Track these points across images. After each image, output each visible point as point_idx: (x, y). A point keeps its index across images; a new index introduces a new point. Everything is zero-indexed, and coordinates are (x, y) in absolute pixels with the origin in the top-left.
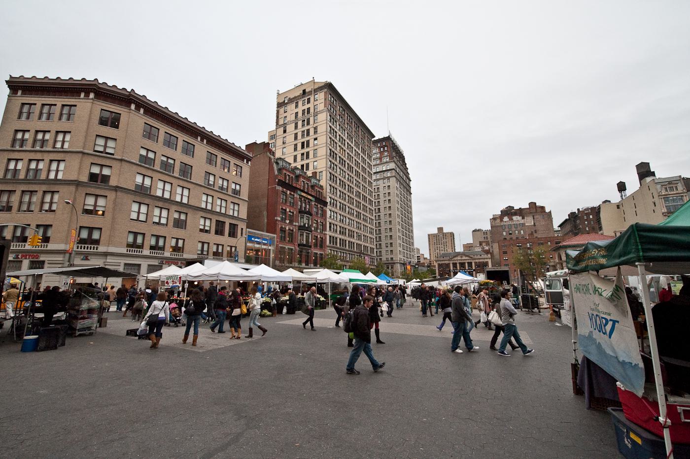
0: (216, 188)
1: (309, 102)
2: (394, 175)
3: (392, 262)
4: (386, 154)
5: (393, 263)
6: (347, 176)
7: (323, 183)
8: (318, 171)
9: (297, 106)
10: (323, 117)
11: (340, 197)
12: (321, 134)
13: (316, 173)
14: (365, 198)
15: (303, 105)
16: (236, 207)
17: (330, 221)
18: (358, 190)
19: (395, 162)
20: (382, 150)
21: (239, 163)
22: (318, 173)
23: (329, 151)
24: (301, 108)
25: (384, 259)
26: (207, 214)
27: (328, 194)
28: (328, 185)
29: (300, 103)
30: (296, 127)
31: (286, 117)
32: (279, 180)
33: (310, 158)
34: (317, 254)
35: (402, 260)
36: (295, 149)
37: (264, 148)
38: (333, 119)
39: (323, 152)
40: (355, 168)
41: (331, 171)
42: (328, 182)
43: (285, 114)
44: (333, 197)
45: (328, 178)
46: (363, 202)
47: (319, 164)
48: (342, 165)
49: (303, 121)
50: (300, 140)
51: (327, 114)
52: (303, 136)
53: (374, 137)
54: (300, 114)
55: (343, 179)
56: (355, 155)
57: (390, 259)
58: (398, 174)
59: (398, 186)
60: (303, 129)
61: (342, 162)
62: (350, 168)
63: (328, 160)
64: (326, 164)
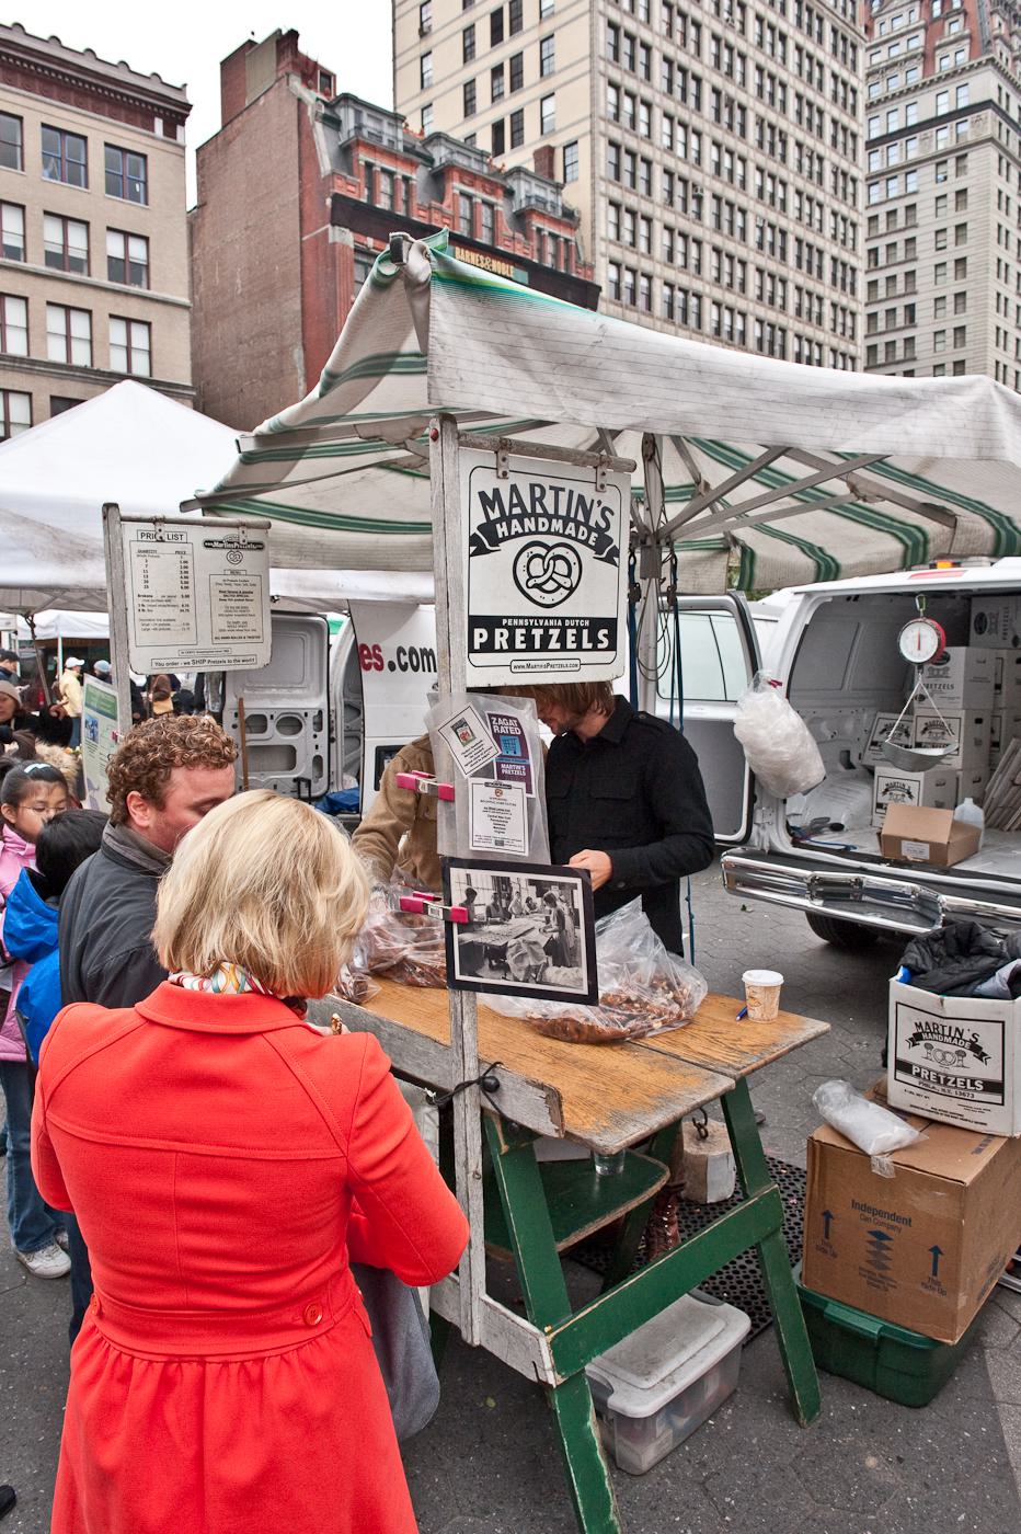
0: (36, 262)
2: (987, 133)
4: (955, 28)
6: (710, 154)
8: (558, 141)
11: (671, 257)
13: (550, 150)
14: (810, 257)
16: (80, 325)
18: (773, 217)
19: (998, 67)
21: (128, 136)
22: (559, 153)
26: (10, 374)
27: (601, 247)
28: (603, 203)
32: (336, 197)
37: (278, 63)
40: (757, 108)
41: (616, 134)
42: (602, 187)
44: (631, 259)
45: (604, 169)
46: (796, 277)
55: (683, 170)
56: (761, 44)
61: (683, 79)
62: (774, 139)
63: (602, 82)
64: (593, 102)
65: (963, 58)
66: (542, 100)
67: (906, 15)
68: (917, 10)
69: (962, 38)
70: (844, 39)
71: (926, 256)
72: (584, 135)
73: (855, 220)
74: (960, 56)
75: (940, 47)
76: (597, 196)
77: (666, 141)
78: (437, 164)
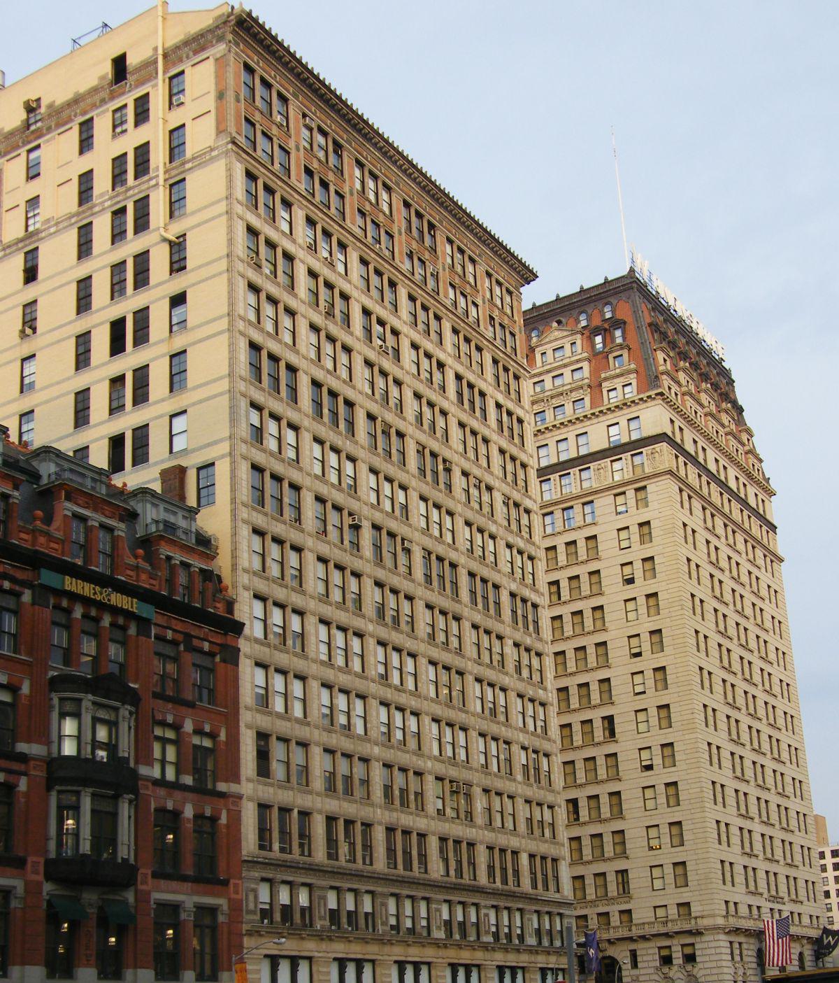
1: (142, 114)
3: (687, 927)
5: (690, 933)
7: (215, 520)
8: (192, 462)
9: (86, 144)
10: (214, 185)
12: (204, 273)
13: (182, 471)
14: (485, 589)
15: (115, 136)
17: (264, 722)
20: (599, 346)
23: (243, 354)
24: (107, 147)
25: (642, 914)
27: (244, 579)
28: (245, 531)
29: (103, 126)
30: (85, 248)
31: (34, 202)
33: (153, 396)
34: (175, 908)
35: (743, 910)
36: (82, 359)
38: (263, 188)
39: (214, 361)
43: (33, 189)
45: (245, 493)
47: (199, 424)
48: (336, 423)
49: (120, 213)
50: (105, 309)
51: (229, 170)
52: (117, 288)
53: (527, 275)
54: (102, 183)
57: (673, 911)
58: (693, 459)
59: (696, 522)
60: (116, 257)
65: (631, 393)
66: (172, 417)
67: (568, 347)
68: (579, 342)
69: (629, 372)
70: (506, 370)
71: (620, 670)
72: (223, 456)
73: (533, 553)
74: (627, 389)
75: (606, 379)
76: (240, 524)
77: (321, 588)
78: (45, 481)
